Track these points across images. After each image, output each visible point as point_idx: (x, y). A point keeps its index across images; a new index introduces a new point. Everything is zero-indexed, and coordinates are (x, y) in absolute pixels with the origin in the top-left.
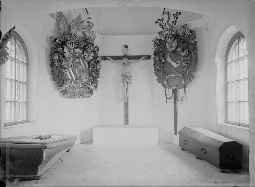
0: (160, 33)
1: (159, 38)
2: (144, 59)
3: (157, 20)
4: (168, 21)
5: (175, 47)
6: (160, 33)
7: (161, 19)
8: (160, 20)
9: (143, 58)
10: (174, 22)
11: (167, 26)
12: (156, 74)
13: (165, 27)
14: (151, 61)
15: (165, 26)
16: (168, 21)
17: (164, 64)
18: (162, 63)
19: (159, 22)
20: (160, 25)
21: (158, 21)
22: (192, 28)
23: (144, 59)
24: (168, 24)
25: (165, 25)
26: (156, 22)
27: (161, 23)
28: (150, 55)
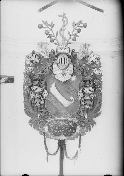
3: (42, 23)
7: (49, 23)
10: (73, 37)
11: (59, 38)
15: (56, 37)
20: (47, 33)
21: (44, 26)
26: (40, 27)
27: (49, 30)
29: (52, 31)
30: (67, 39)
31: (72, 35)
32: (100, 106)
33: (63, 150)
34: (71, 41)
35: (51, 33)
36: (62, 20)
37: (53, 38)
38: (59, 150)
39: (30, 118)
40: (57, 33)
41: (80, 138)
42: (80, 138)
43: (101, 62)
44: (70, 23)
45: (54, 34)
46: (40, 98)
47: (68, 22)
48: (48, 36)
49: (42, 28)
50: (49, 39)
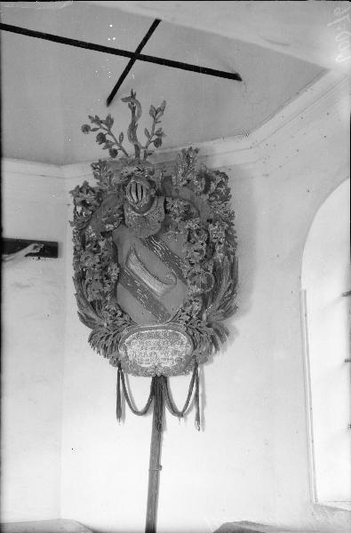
0: (99, 166)
1: (93, 183)
2: (31, 254)
3: (88, 122)
4: (133, 127)
5: (159, 226)
6: (99, 166)
7: (103, 118)
8: (102, 122)
9: (29, 249)
10: (155, 138)
11: (129, 147)
12: (86, 320)
13: (121, 148)
14: (66, 264)
15: (119, 145)
16: (133, 127)
17: (117, 281)
18: (108, 277)
19: (95, 130)
20: (101, 138)
21: (93, 126)
22: (216, 164)
23: (31, 254)
24: (133, 138)
25: (121, 141)
26: (86, 129)
27: (105, 132)
28: (56, 243)
29: (110, 133)
30: (144, 145)
31: (153, 134)
32: (233, 287)
33: (162, 401)
34: (152, 147)
35: (108, 137)
36: (130, 106)
37: (115, 147)
38: (153, 404)
39: (89, 331)
40: (122, 134)
41: (195, 374)
42: (195, 374)
43: (229, 186)
44: (145, 111)
45: (115, 139)
46: (102, 280)
47: (140, 112)
48: (104, 144)
49: (90, 132)
50: (107, 150)
